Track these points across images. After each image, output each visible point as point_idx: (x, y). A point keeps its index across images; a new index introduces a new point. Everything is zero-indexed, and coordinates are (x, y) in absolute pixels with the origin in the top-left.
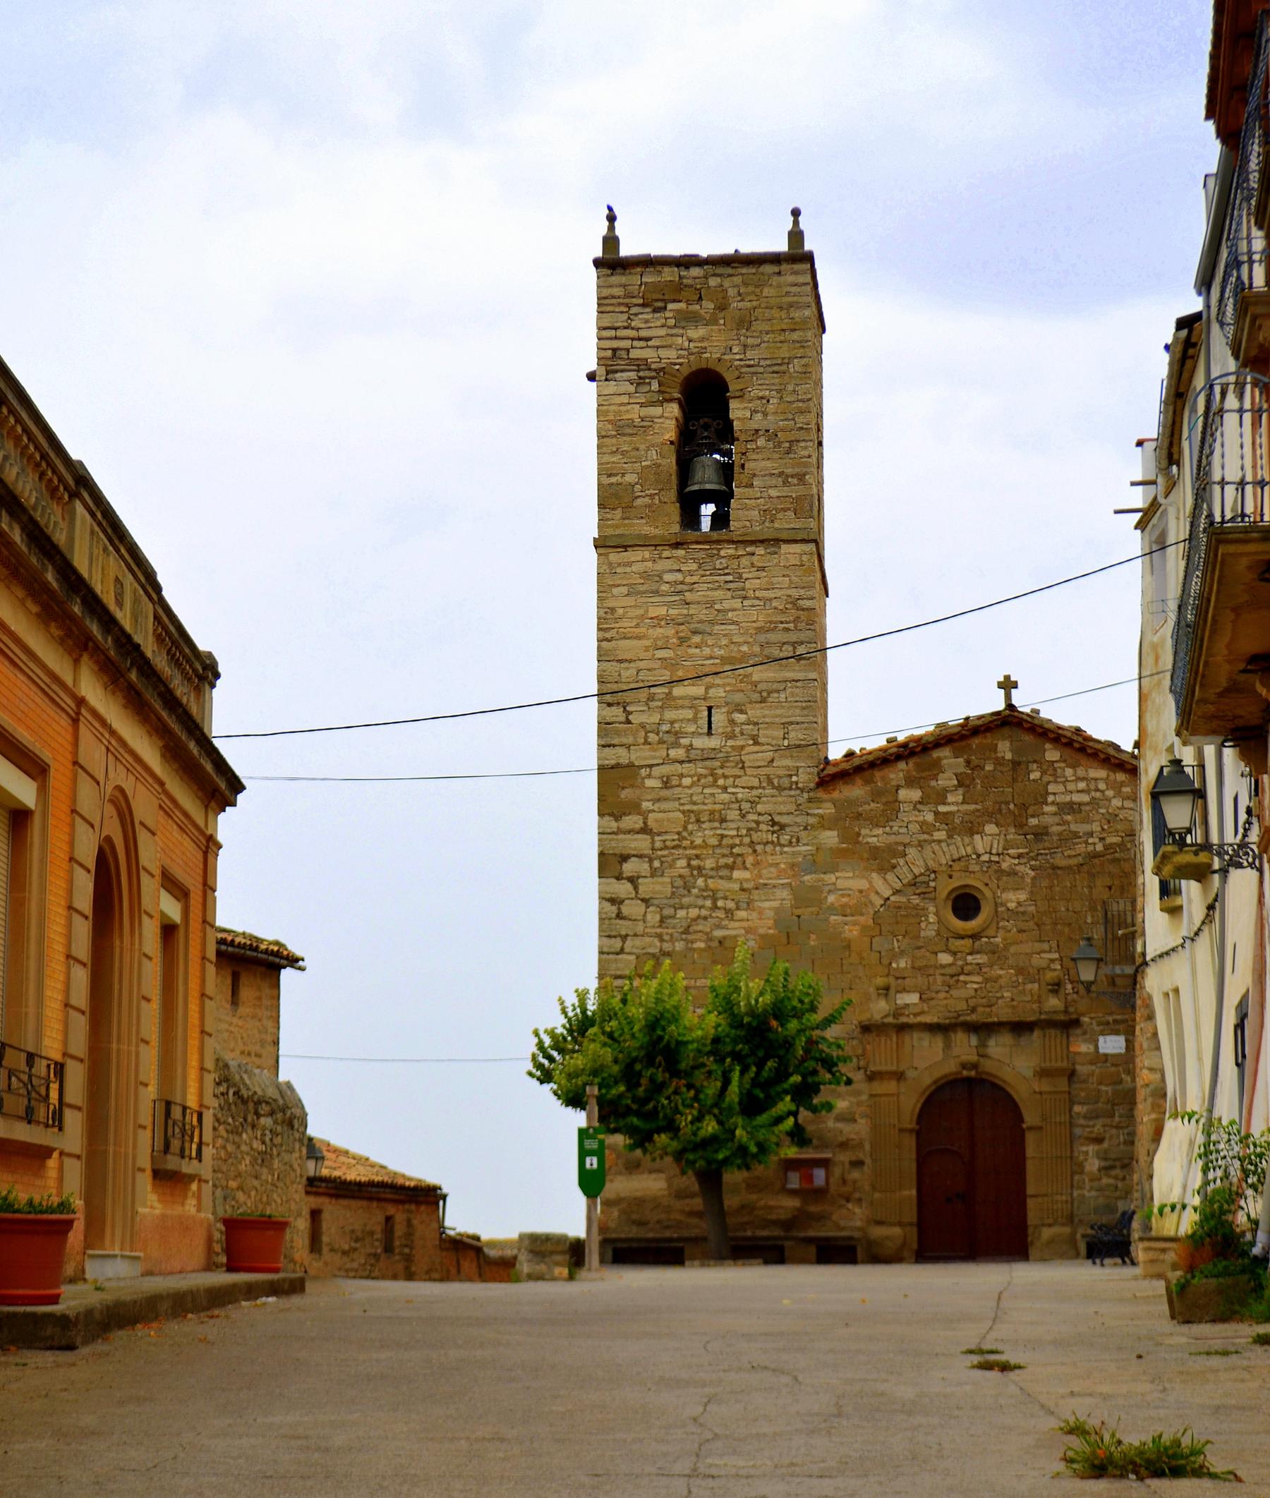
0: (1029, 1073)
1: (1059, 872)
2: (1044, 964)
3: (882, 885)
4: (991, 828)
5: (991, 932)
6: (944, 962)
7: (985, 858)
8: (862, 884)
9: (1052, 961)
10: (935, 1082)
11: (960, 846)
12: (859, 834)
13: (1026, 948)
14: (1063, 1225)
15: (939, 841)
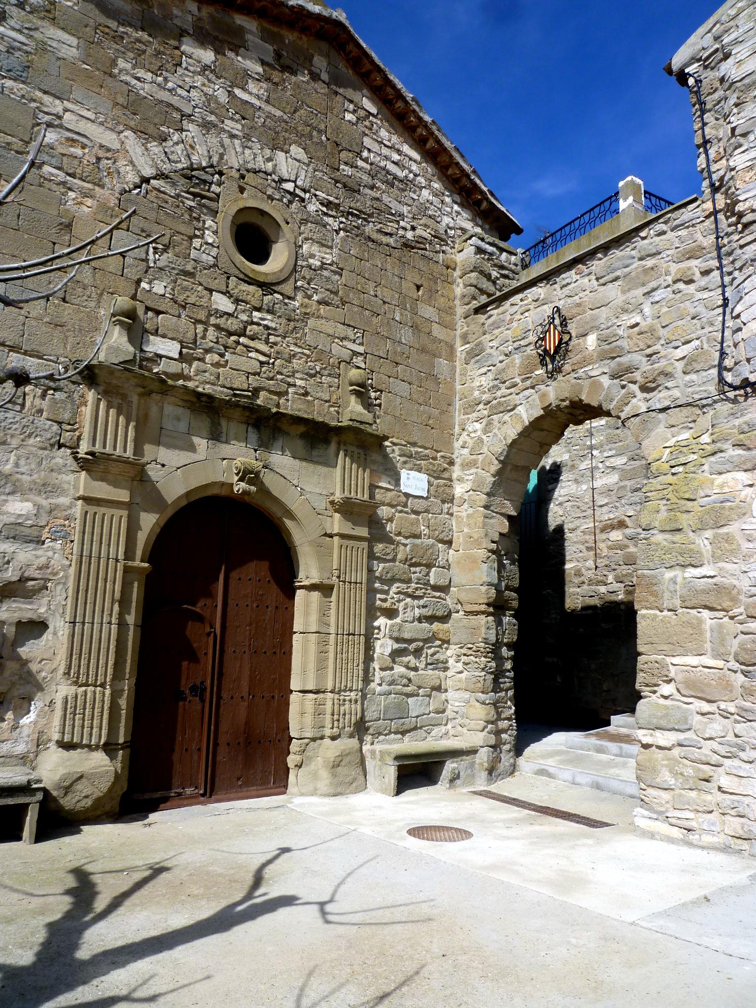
0: (322, 504)
1: (370, 244)
2: (346, 354)
3: (140, 158)
4: (296, 150)
5: (287, 288)
6: (222, 308)
7: (289, 186)
8: (109, 139)
9: (355, 353)
10: (188, 494)
11: (256, 156)
12: (114, 63)
13: (329, 327)
14: (351, 736)
15: (233, 136)
